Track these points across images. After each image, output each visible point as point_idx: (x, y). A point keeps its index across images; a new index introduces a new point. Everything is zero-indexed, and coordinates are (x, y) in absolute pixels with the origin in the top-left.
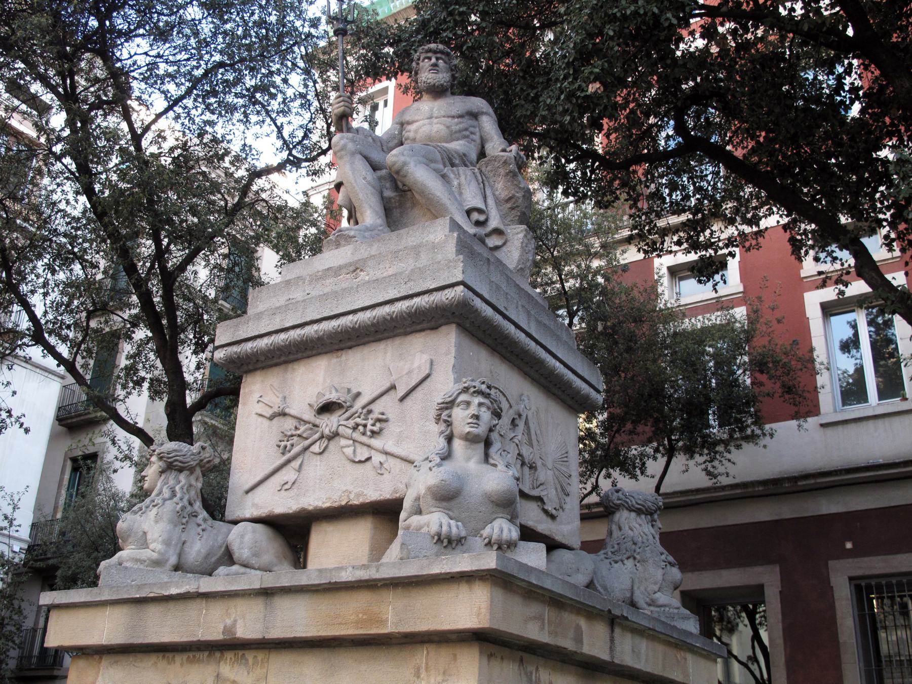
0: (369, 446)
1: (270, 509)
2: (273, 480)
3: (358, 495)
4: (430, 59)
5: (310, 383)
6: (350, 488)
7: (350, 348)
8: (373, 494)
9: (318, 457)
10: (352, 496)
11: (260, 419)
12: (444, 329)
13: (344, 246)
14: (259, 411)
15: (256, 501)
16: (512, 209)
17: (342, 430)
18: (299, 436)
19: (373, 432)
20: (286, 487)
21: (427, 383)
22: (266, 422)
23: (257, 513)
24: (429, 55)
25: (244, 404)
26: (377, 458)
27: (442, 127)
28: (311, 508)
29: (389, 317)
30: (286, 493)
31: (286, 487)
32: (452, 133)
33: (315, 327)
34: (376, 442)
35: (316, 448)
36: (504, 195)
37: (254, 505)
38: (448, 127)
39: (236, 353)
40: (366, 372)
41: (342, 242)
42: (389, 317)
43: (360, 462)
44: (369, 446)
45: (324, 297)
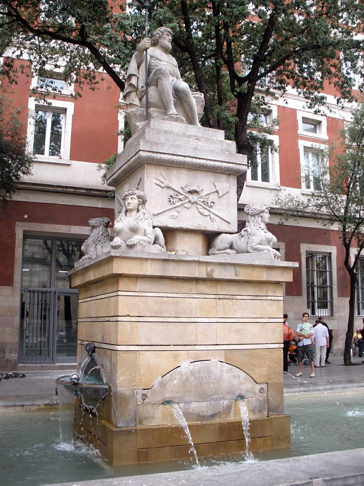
0: (209, 211)
1: (166, 224)
2: (167, 213)
4: (168, 35)
6: (201, 224)
10: (202, 227)
11: (157, 186)
13: (179, 122)
15: (160, 219)
19: (211, 206)
20: (173, 217)
22: (160, 189)
23: (160, 225)
24: (169, 34)
26: (212, 216)
27: (172, 69)
28: (185, 228)
30: (173, 220)
31: (173, 217)
37: (158, 221)
43: (206, 215)
44: (209, 211)
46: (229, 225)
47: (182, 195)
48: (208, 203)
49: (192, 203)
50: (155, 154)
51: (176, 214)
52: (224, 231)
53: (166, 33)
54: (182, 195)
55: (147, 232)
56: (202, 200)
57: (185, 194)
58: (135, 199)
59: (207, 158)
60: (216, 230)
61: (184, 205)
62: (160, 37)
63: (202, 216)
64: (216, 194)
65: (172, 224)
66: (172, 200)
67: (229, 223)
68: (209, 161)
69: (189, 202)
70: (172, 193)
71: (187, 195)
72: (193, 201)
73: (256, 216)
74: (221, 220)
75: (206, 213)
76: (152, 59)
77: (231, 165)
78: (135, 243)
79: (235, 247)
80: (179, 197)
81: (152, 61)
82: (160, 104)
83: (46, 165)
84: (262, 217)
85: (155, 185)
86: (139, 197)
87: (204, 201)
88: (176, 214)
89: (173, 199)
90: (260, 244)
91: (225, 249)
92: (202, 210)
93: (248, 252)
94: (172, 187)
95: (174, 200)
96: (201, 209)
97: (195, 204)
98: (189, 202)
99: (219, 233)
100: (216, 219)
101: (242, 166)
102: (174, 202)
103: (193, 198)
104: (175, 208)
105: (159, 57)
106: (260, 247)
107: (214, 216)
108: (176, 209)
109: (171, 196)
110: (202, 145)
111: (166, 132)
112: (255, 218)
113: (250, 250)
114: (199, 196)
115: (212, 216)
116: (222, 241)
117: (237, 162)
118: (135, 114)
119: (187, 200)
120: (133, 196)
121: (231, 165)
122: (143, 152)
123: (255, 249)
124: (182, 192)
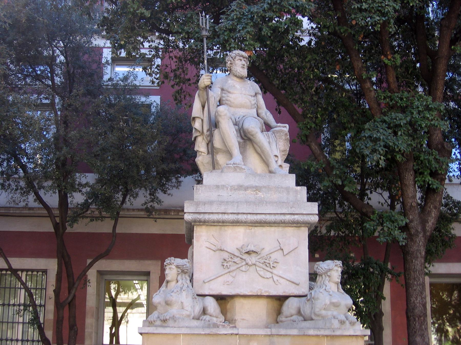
1: (220, 292)
2: (219, 279)
3: (266, 292)
4: (241, 60)
5: (236, 238)
7: (256, 226)
8: (274, 292)
9: (244, 273)
10: (263, 291)
11: (209, 250)
12: (303, 228)
13: (238, 172)
14: (207, 246)
16: (284, 155)
17: (257, 263)
18: (234, 262)
19: (273, 267)
20: (228, 283)
21: (296, 250)
22: (212, 252)
23: (212, 293)
24: (241, 58)
25: (198, 241)
27: (248, 101)
29: (283, 221)
31: (228, 283)
32: (252, 105)
33: (245, 216)
34: (274, 271)
35: (243, 268)
36: (282, 148)
38: (250, 101)
39: (198, 218)
40: (266, 239)
41: (238, 170)
42: (283, 221)
44: (272, 273)
45: (248, 202)
46: (297, 287)
47: (238, 257)
48: (269, 263)
49: (250, 266)
50: (202, 215)
51: (231, 279)
52: (292, 295)
53: (238, 58)
54: (238, 257)
55: (185, 304)
56: (262, 261)
57: (241, 256)
58: (173, 269)
59: (265, 212)
60: (281, 294)
61: (241, 268)
62: (231, 64)
63: (263, 279)
64: (281, 251)
65: (225, 291)
66: (225, 264)
67: (298, 285)
68: (268, 215)
69: (247, 264)
70: (226, 255)
71: (244, 257)
72: (250, 263)
73: (323, 276)
74: (287, 282)
75: (269, 275)
76: (223, 92)
77: (296, 217)
78: (168, 317)
79: (302, 313)
80: (233, 260)
81: (223, 95)
82: (224, 149)
83: (138, 219)
84: (329, 276)
85: (206, 249)
86: (177, 267)
87: (265, 262)
88: (231, 279)
89: (227, 263)
90: (324, 309)
91: (292, 316)
92: (262, 273)
93: (312, 319)
94: (225, 249)
95: (228, 265)
96: (261, 271)
97: (254, 266)
98: (247, 264)
99: (286, 298)
100: (281, 280)
101: (311, 216)
102: (229, 267)
103: (252, 259)
104: (229, 272)
105: (230, 90)
106: (323, 312)
107: (278, 278)
108: (231, 274)
109: (225, 260)
110: (263, 196)
111: (218, 187)
112: (322, 278)
113: (314, 317)
114: (259, 257)
115: (275, 278)
116: (290, 306)
117: (304, 213)
118: (202, 163)
119: (244, 263)
120: (170, 266)
121: (296, 217)
122: (188, 214)
123: (318, 316)
124: (237, 253)
